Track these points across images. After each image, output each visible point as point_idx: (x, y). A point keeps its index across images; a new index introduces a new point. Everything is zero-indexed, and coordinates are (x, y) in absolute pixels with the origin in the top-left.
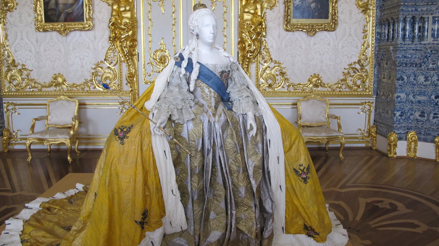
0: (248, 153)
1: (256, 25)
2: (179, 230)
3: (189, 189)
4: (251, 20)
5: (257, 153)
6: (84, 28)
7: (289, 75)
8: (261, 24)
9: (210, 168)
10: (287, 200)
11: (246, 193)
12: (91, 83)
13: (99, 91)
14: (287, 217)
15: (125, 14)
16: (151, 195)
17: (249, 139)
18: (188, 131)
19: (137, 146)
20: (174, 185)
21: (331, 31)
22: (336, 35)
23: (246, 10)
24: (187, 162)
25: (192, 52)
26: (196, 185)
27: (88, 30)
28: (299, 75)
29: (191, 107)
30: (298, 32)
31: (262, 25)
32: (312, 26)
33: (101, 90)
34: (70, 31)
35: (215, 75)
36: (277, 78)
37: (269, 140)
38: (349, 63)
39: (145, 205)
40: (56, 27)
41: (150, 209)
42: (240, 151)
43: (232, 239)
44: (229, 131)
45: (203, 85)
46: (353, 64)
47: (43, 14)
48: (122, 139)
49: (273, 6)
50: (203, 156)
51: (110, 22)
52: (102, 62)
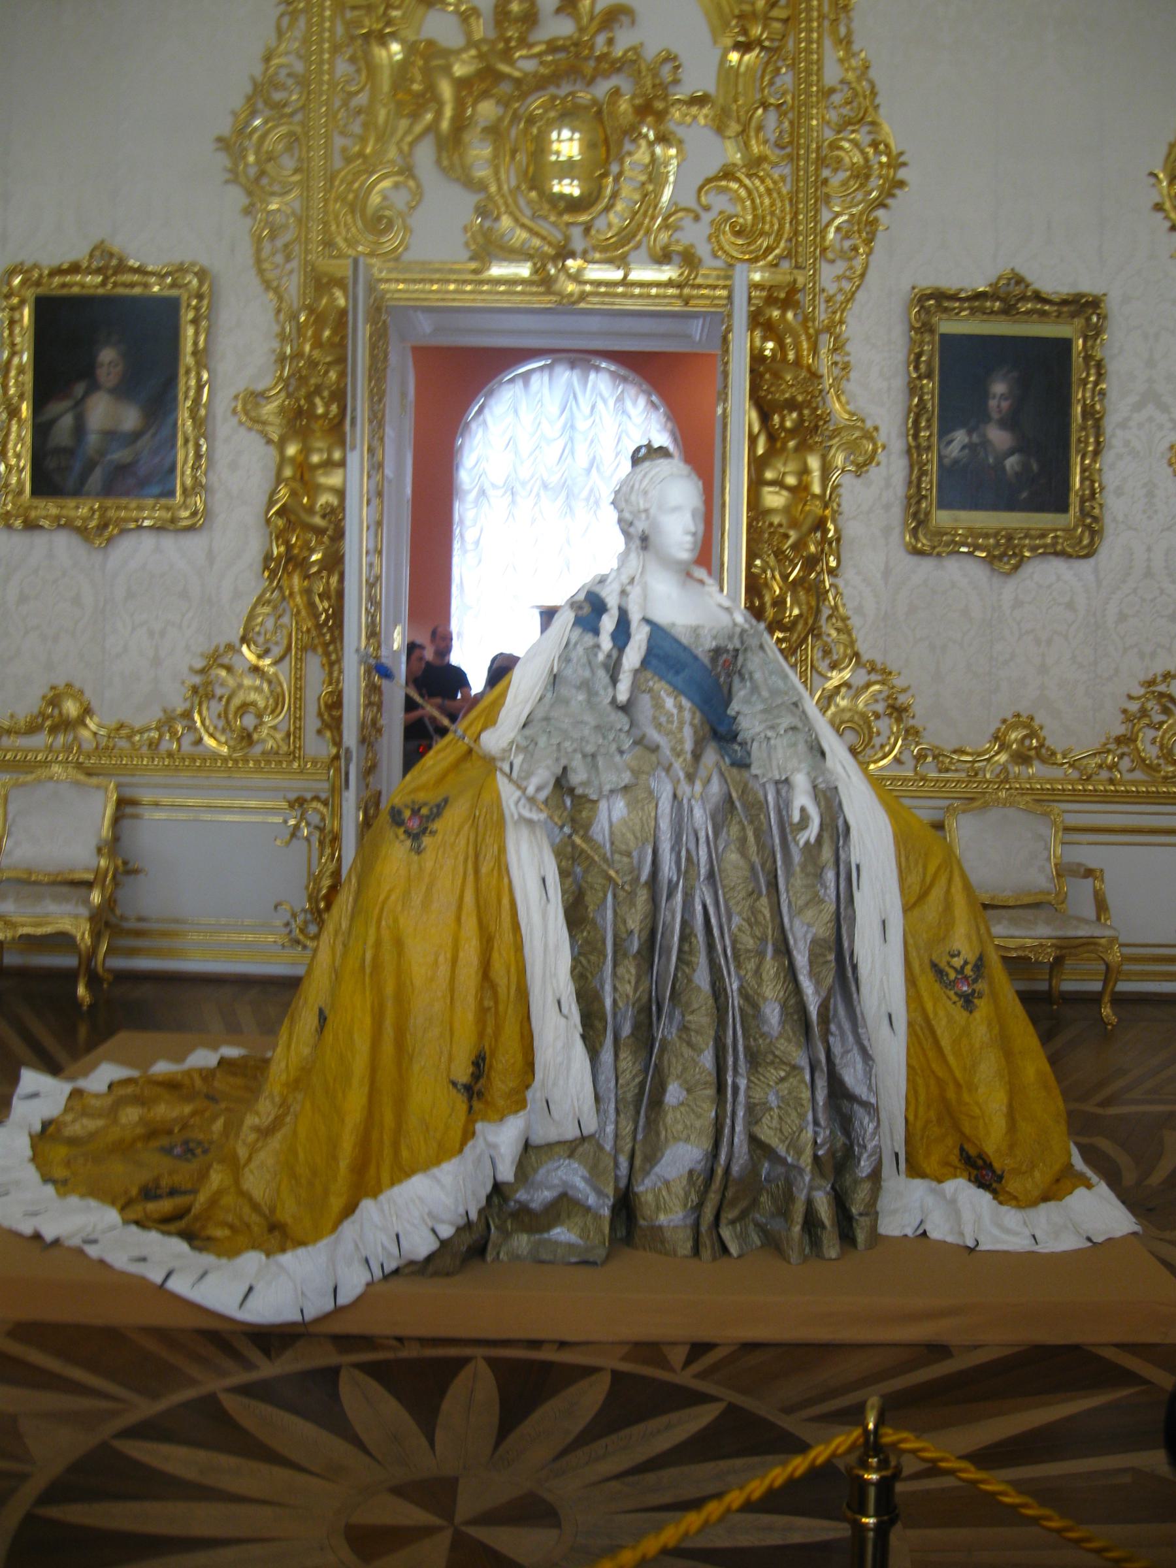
0: (793, 899)
1: (805, 528)
2: (571, 1133)
3: (608, 1003)
4: (787, 510)
5: (822, 901)
6: (173, 520)
7: (920, 714)
8: (820, 525)
9: (676, 939)
10: (914, 1063)
11: (782, 1023)
12: (185, 722)
13: (215, 756)
14: (911, 1118)
15: (326, 474)
16: (501, 1008)
17: (797, 858)
18: (611, 825)
19: (461, 858)
20: (565, 986)
21: (1079, 557)
22: (1096, 571)
23: (769, 475)
24: (604, 918)
25: (629, 588)
26: (629, 989)
27: (191, 528)
28: (958, 718)
29: (621, 752)
30: (955, 557)
31: (825, 531)
32: (1010, 538)
33: (225, 750)
34: (123, 531)
35: (696, 658)
36: (876, 726)
37: (858, 867)
38: (1142, 677)
39: (481, 1035)
40: (72, 513)
41: (493, 1054)
42: (767, 889)
43: (735, 1169)
44: (734, 830)
45: (661, 688)
46: (1159, 679)
47: (28, 468)
48: (415, 837)
49: (865, 464)
50: (654, 900)
51: (271, 503)
52: (230, 647)
